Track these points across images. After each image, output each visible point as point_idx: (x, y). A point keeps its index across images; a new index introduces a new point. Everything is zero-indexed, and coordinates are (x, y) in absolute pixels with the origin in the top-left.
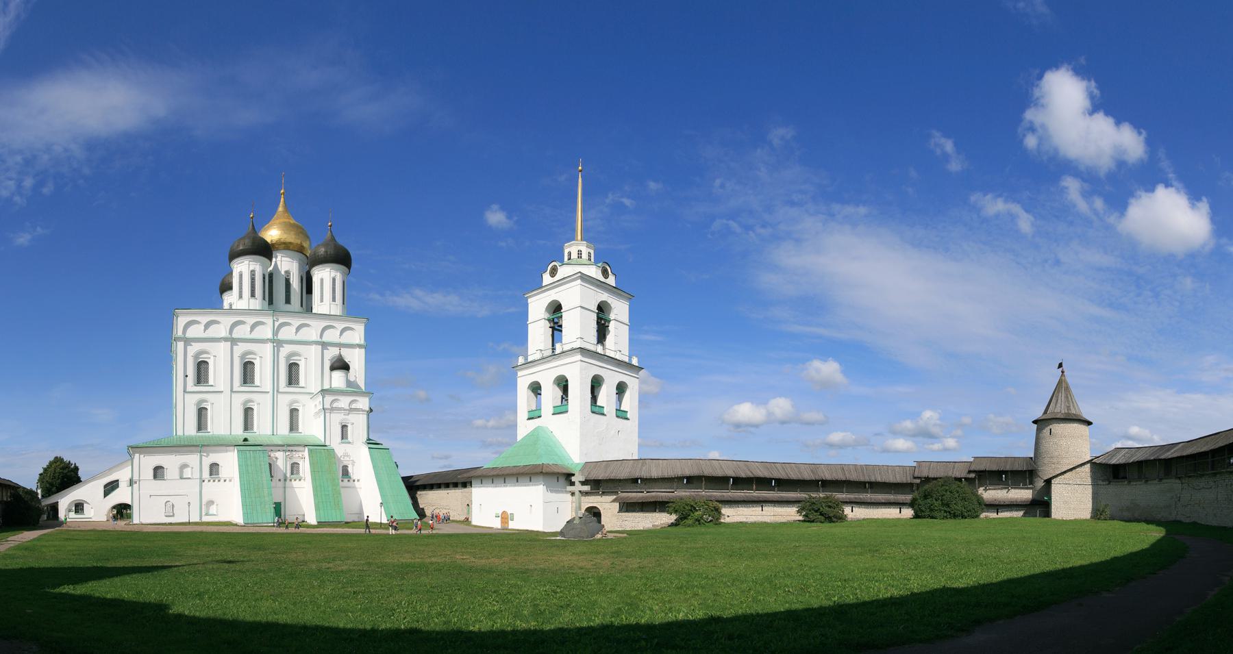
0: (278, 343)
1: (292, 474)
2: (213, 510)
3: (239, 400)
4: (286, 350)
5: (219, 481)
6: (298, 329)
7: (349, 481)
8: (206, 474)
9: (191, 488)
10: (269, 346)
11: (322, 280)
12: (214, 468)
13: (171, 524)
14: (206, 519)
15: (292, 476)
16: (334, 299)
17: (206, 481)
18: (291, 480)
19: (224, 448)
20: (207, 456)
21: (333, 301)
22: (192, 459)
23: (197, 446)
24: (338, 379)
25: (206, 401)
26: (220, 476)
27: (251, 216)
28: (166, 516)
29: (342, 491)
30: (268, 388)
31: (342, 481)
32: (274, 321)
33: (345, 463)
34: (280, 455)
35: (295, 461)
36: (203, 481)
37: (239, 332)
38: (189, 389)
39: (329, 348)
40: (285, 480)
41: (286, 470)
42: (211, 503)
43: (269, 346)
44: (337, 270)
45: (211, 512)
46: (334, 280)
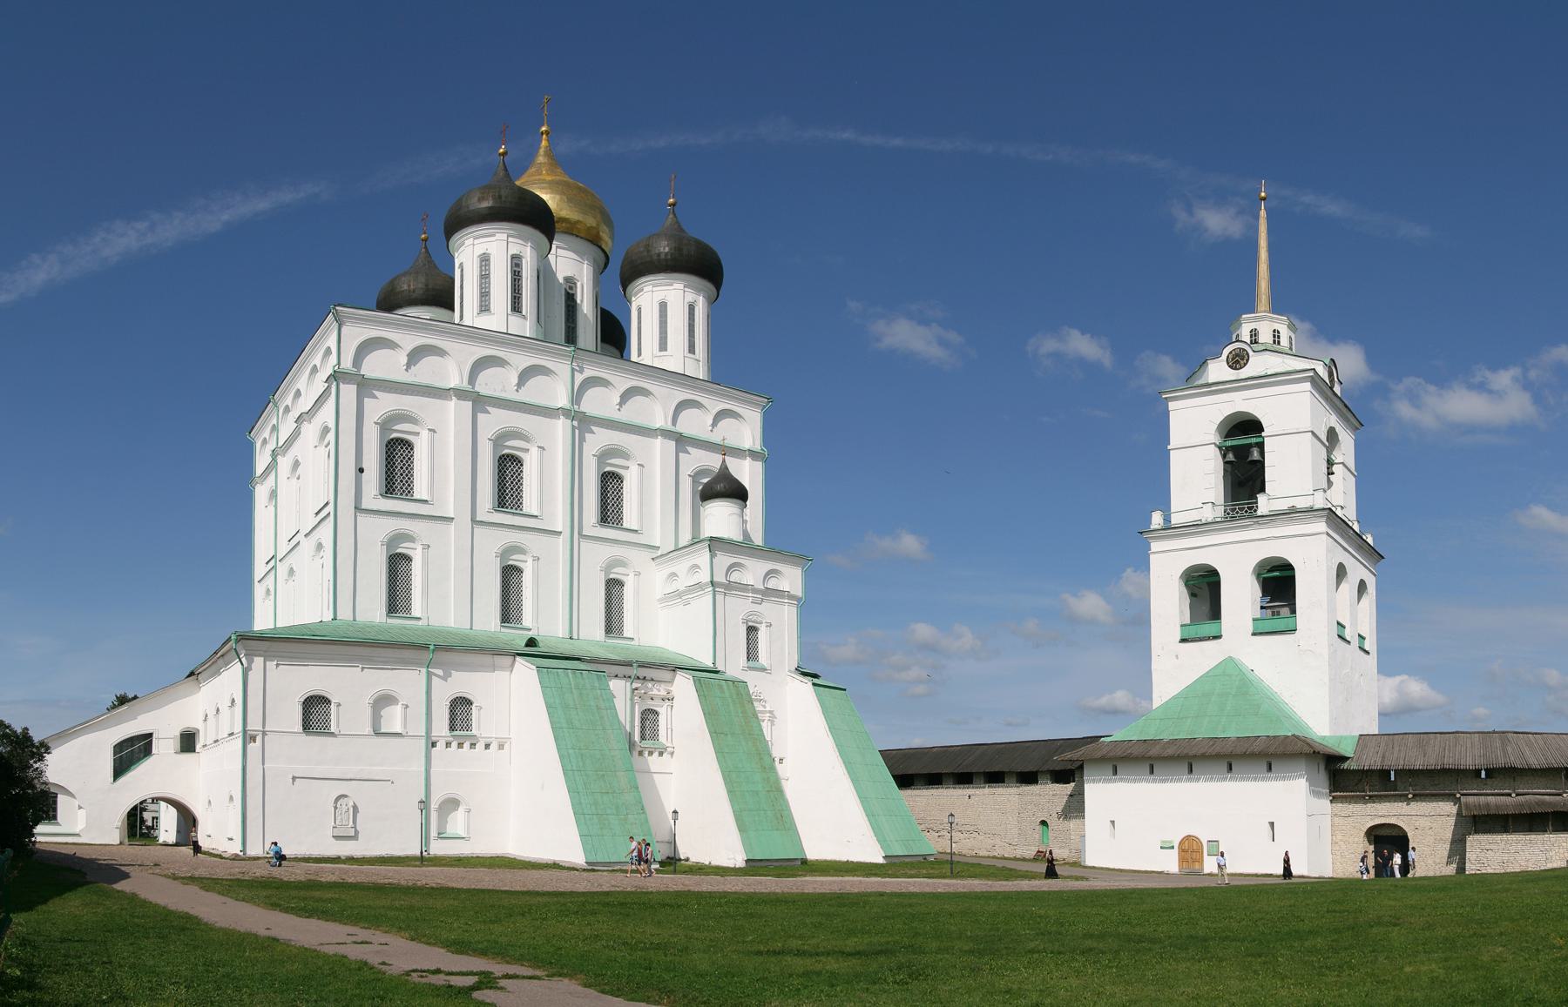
0: (583, 423)
1: (643, 738)
2: (457, 823)
3: (491, 544)
4: (599, 439)
5: (473, 745)
6: (626, 396)
9: (404, 761)
13: (351, 860)
14: (438, 848)
15: (646, 744)
16: (692, 349)
17: (441, 745)
19: (487, 659)
20: (445, 678)
21: (690, 352)
22: (407, 682)
23: (425, 647)
24: (720, 518)
25: (411, 539)
26: (474, 732)
27: (501, 151)
28: (337, 837)
30: (559, 519)
32: (573, 370)
34: (618, 687)
35: (650, 705)
36: (434, 745)
37: (490, 382)
38: (367, 503)
39: (689, 449)
41: (633, 726)
42: (451, 804)
43: (561, 427)
44: (698, 290)
45: (450, 831)
46: (692, 308)
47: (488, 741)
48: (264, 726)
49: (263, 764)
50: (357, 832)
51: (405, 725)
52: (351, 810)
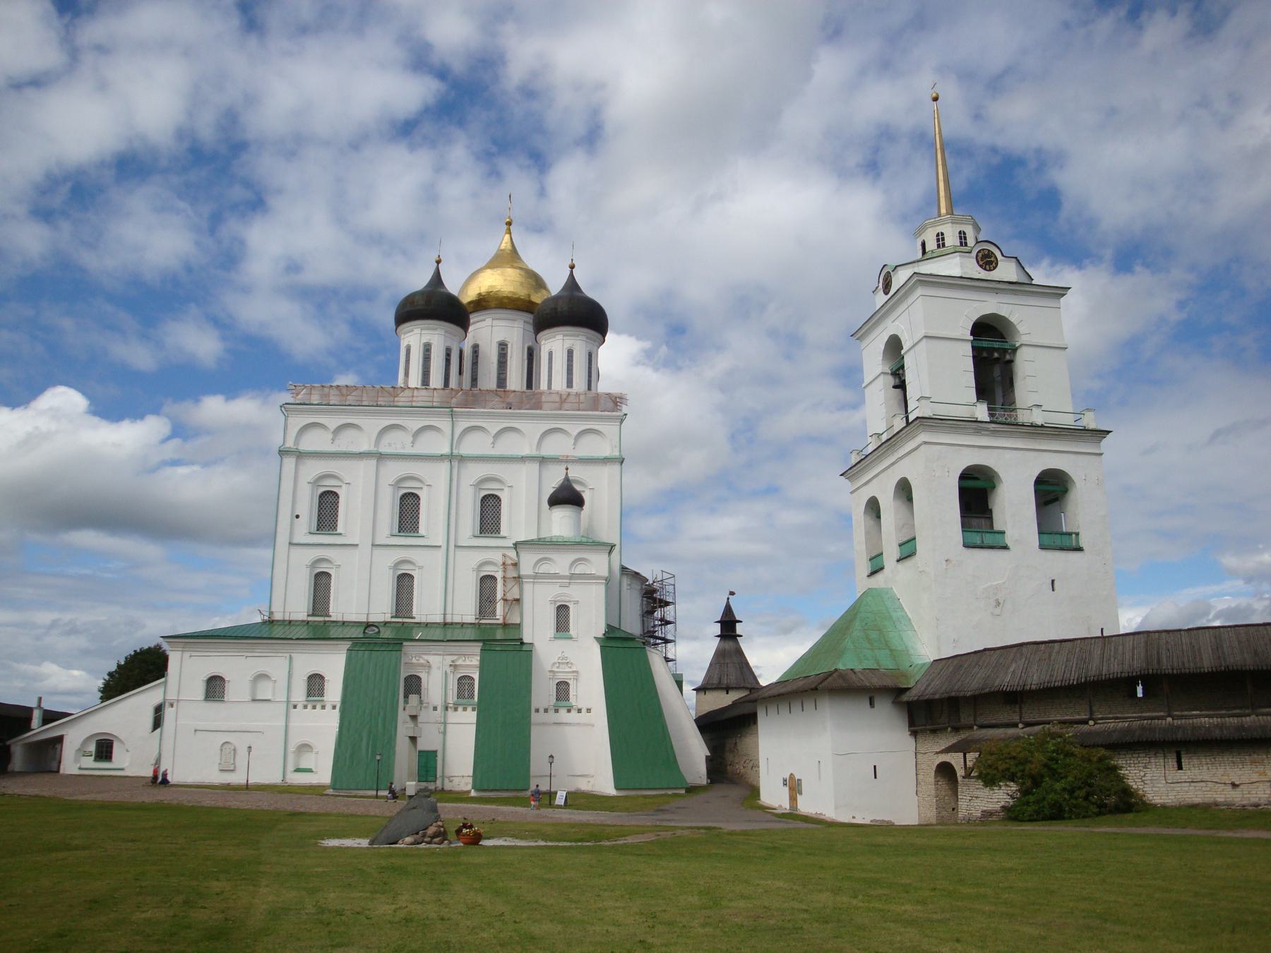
5: (323, 707)
7: (569, 711)
8: (299, 693)
9: (269, 719)
10: (445, 466)
11: (551, 354)
12: (316, 684)
17: (300, 706)
18: (456, 709)
24: (561, 522)
26: (325, 698)
29: (533, 729)
31: (557, 711)
33: (561, 677)
36: (295, 707)
40: (447, 708)
46: (570, 353)
47: (335, 703)
48: (178, 697)
49: (176, 721)
50: (235, 767)
51: (274, 694)
52: (232, 752)
